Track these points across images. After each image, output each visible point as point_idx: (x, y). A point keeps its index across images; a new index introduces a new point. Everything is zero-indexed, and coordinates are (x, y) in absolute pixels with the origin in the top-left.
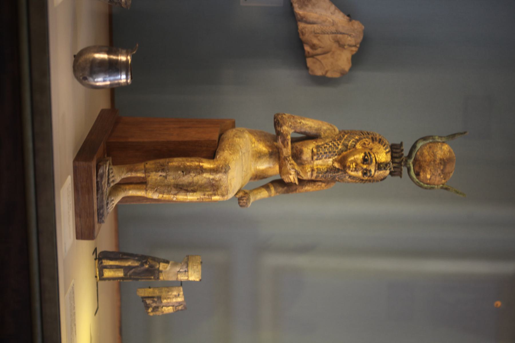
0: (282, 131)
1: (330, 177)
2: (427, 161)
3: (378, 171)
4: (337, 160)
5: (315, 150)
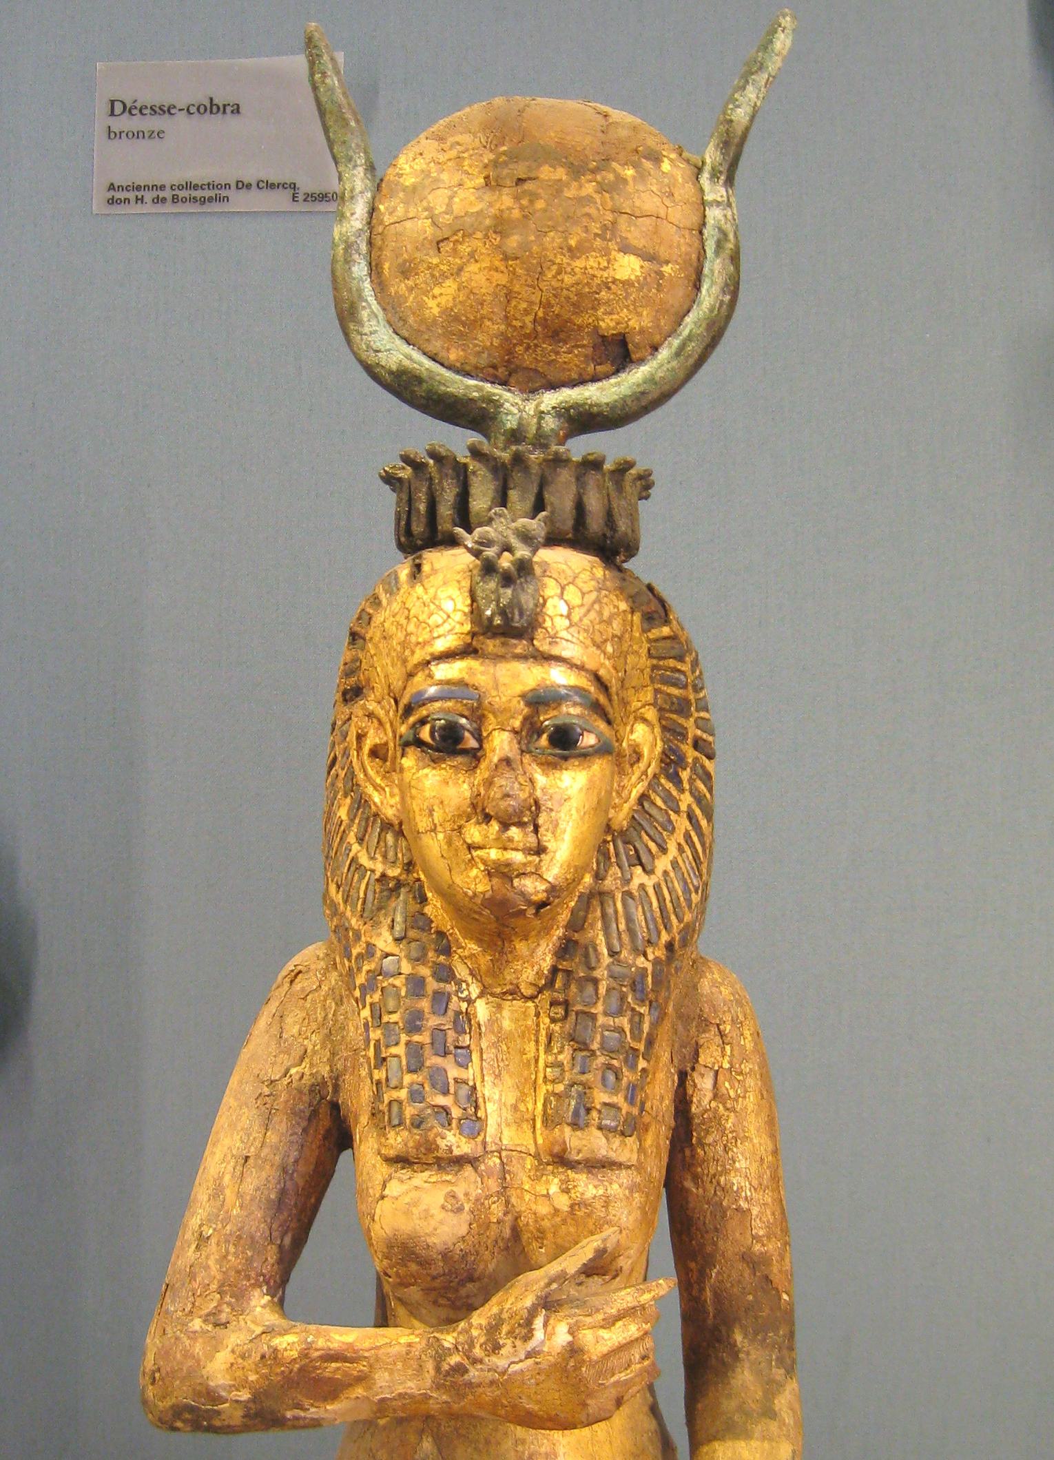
0: (245, 1395)
1: (624, 1022)
2: (503, 279)
3: (540, 633)
4: (485, 960)
5: (397, 1141)
